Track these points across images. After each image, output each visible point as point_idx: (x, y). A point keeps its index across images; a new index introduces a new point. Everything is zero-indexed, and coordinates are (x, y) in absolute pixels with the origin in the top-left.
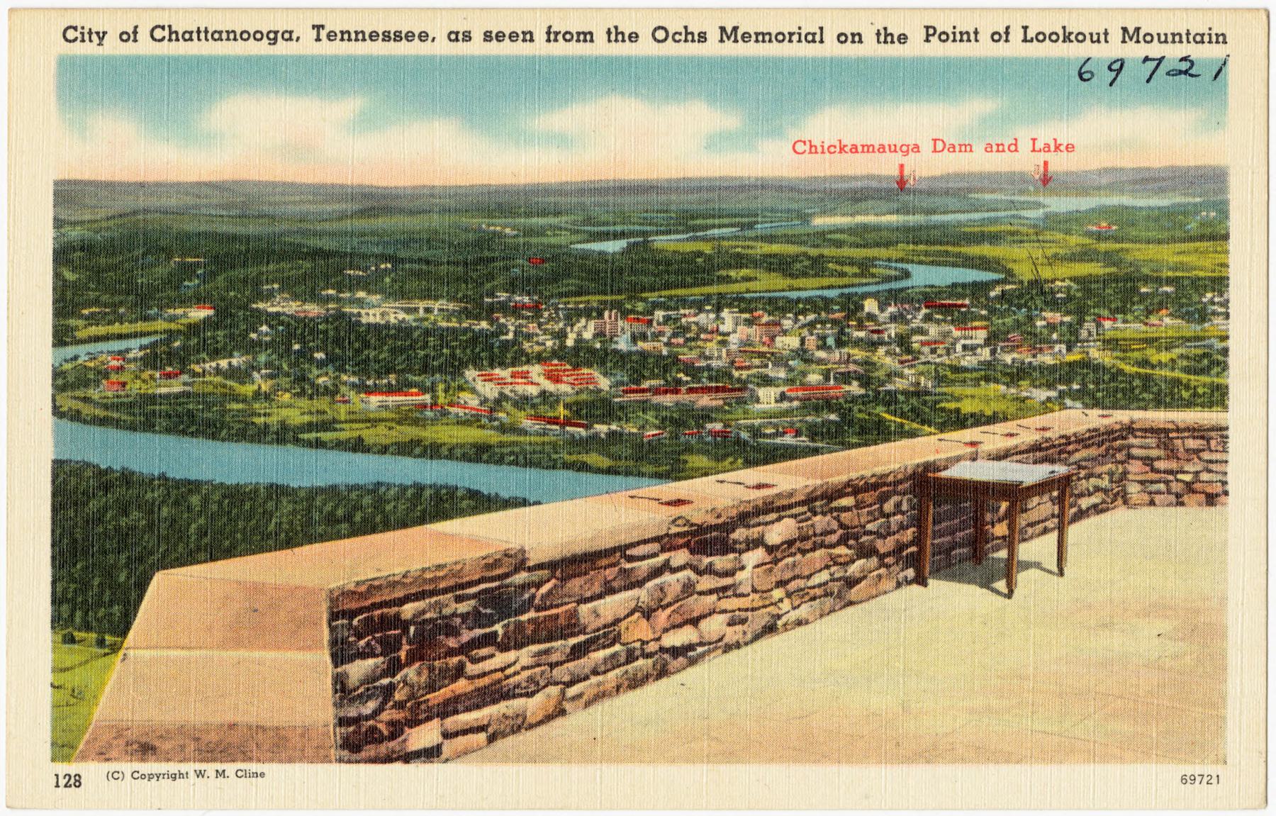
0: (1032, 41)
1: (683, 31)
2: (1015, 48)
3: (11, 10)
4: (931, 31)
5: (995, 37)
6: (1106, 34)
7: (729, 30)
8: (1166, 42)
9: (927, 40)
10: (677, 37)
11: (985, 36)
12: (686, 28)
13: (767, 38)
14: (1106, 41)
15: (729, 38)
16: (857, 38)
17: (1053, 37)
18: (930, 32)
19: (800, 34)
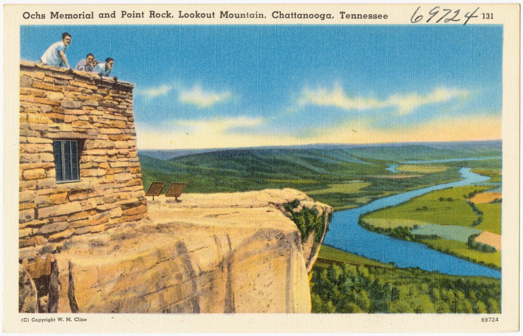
0: (183, 17)
1: (35, 14)
3: (4, 5)
4: (124, 13)
6: (213, 14)
7: (55, 14)
8: (238, 17)
9: (123, 17)
12: (37, 13)
14: (143, 17)
17: (192, 16)
18: (124, 13)
19: (83, 15)
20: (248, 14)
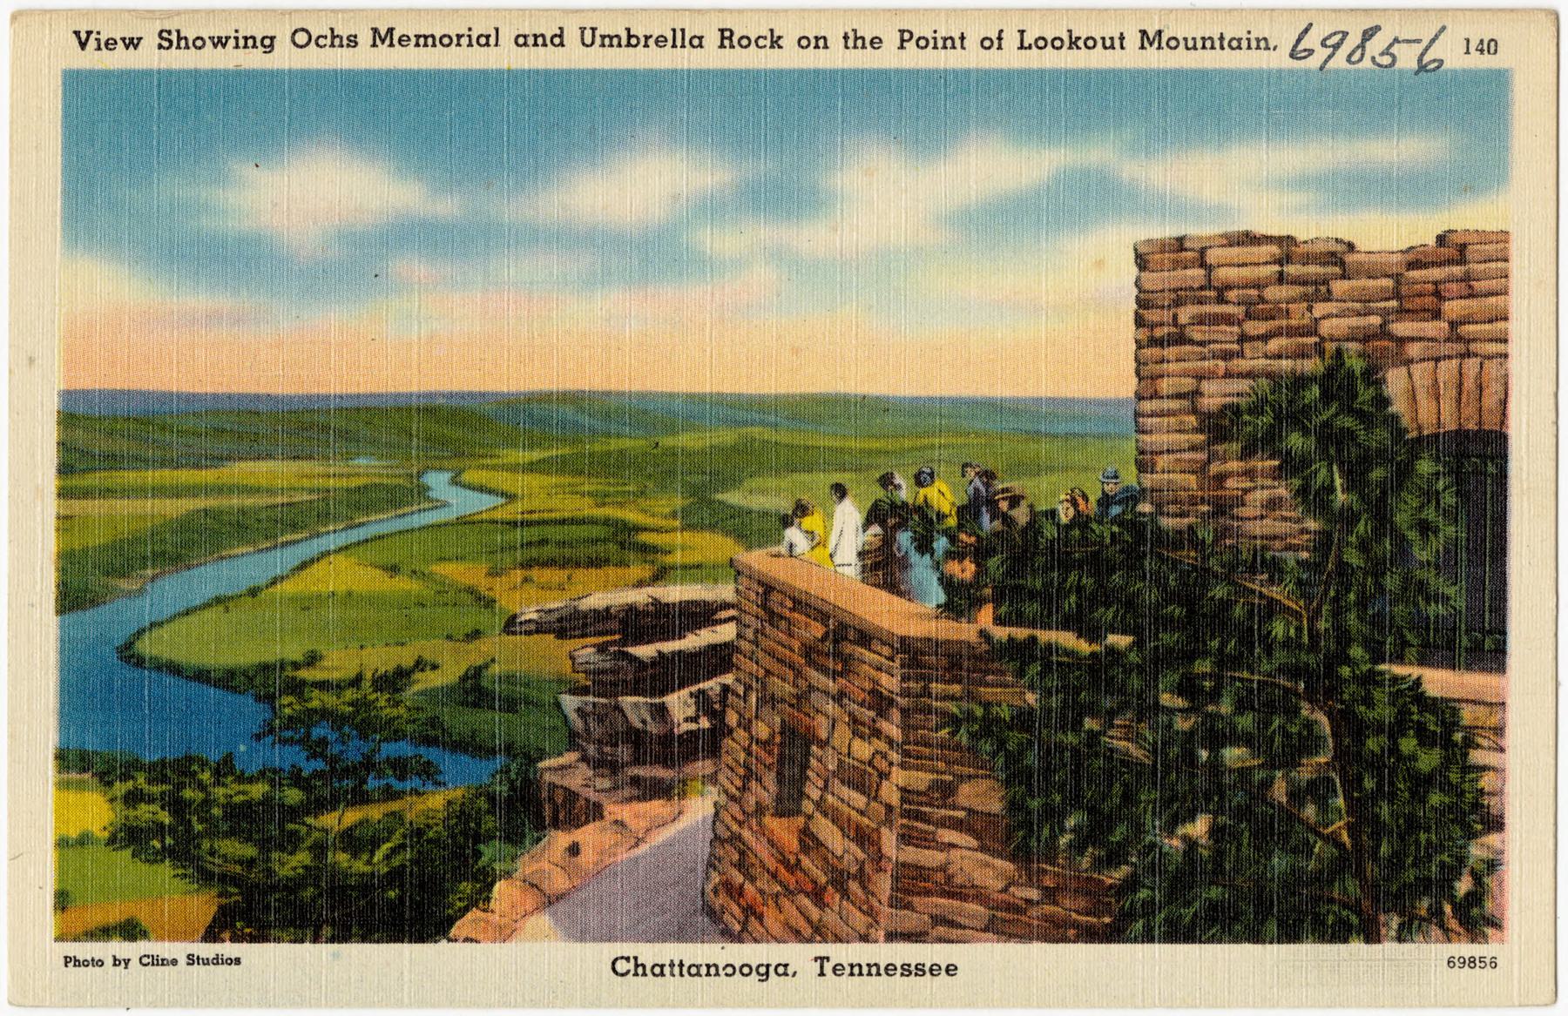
0: (1030, 47)
2: (1009, 58)
4: (907, 36)
5: (986, 43)
6: (1122, 38)
8: (1195, 48)
9: (902, 47)
10: (322, 42)
11: (972, 42)
13: (430, 41)
15: (383, 41)
16: (821, 42)
17: (1056, 43)
18: (905, 37)
20: (1222, 38)
